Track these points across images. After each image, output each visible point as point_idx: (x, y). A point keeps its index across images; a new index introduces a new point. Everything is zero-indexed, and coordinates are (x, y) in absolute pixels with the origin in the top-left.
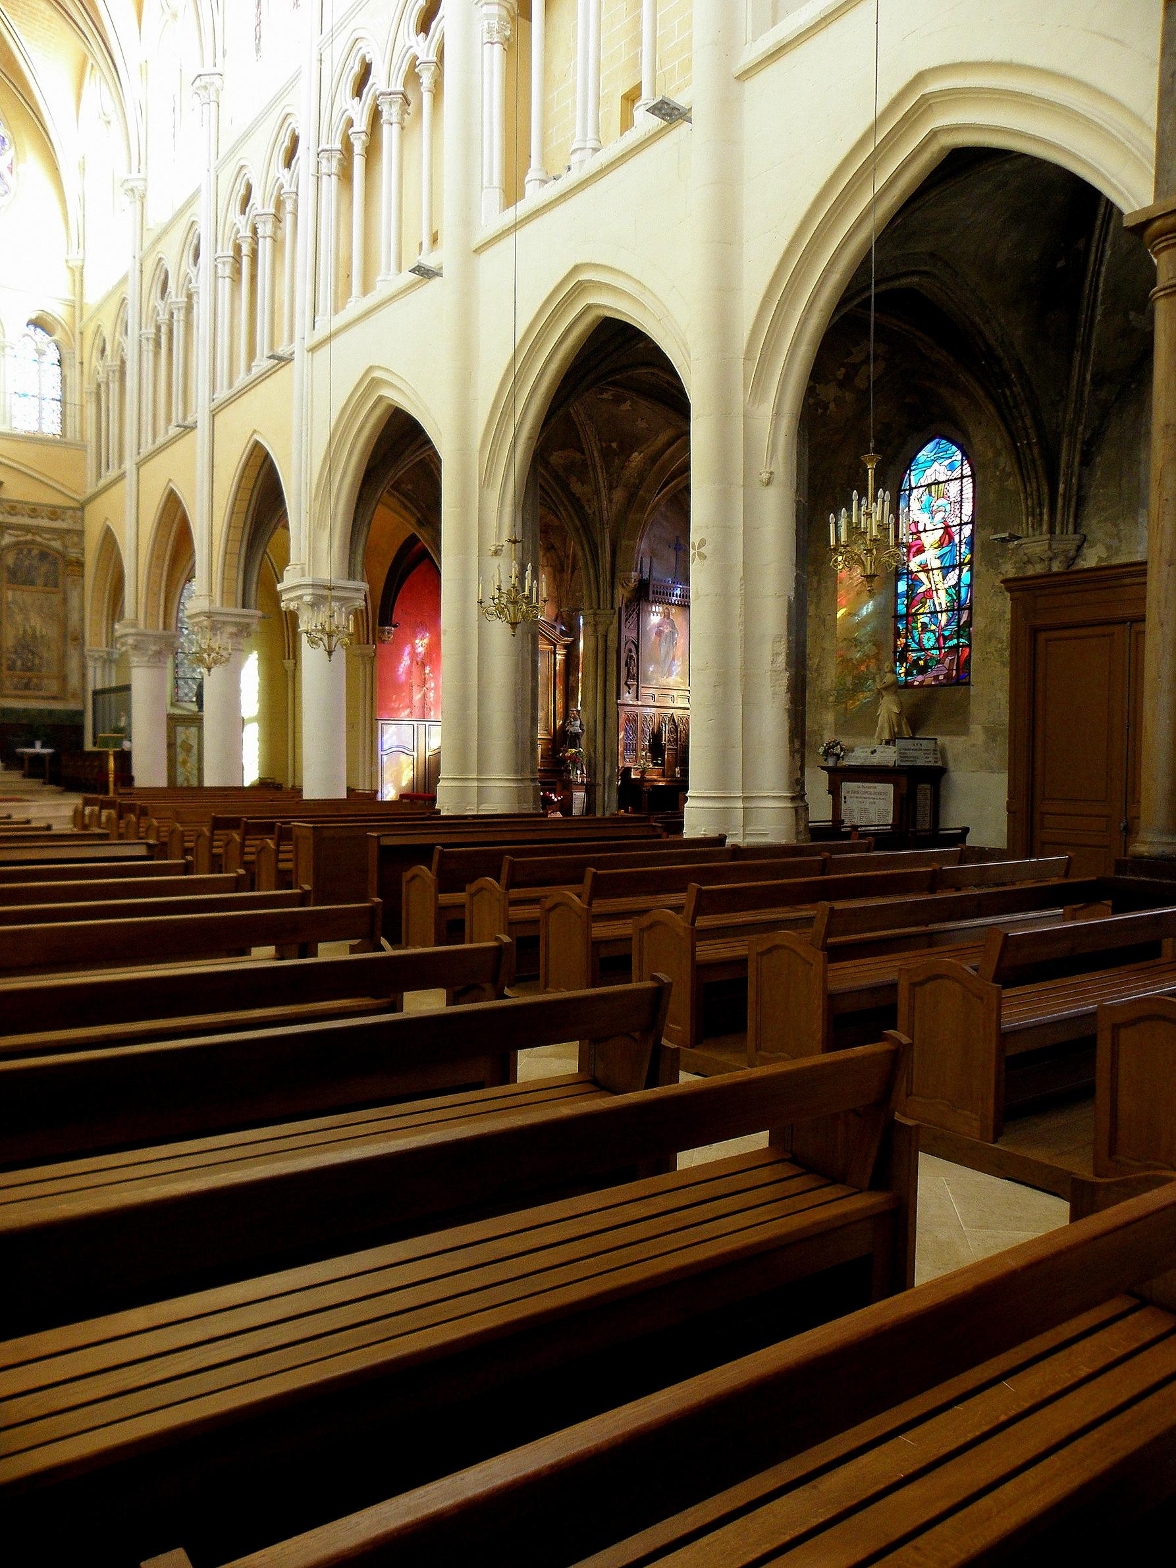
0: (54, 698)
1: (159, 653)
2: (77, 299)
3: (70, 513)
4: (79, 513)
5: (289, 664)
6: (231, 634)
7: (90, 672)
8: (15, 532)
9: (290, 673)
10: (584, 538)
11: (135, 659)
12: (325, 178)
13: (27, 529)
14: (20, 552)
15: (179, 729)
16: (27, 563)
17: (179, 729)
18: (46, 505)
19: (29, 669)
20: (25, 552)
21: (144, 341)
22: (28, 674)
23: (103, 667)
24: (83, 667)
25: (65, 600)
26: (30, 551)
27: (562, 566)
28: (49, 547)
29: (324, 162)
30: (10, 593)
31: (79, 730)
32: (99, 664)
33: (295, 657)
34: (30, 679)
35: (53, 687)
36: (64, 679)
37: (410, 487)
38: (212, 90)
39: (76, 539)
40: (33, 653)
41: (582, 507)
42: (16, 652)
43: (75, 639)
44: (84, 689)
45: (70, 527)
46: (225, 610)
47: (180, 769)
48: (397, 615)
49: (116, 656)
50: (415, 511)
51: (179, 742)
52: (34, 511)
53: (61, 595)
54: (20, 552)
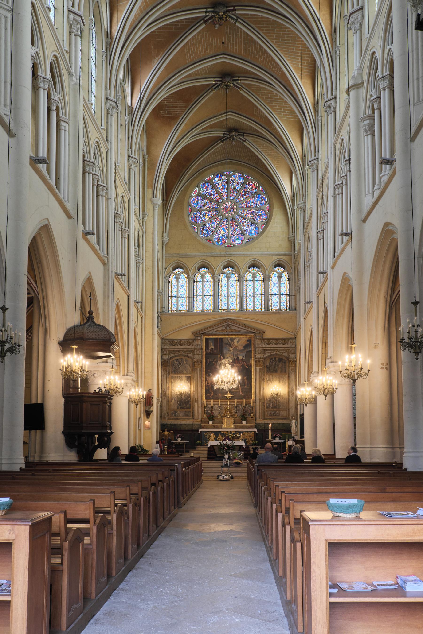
2: (293, 253)
3: (290, 340)
4: (294, 340)
12: (337, 196)
14: (272, 359)
16: (274, 363)
20: (273, 359)
21: (306, 267)
26: (275, 358)
28: (283, 355)
29: (337, 190)
38: (315, 165)
52: (277, 341)
54: (272, 359)
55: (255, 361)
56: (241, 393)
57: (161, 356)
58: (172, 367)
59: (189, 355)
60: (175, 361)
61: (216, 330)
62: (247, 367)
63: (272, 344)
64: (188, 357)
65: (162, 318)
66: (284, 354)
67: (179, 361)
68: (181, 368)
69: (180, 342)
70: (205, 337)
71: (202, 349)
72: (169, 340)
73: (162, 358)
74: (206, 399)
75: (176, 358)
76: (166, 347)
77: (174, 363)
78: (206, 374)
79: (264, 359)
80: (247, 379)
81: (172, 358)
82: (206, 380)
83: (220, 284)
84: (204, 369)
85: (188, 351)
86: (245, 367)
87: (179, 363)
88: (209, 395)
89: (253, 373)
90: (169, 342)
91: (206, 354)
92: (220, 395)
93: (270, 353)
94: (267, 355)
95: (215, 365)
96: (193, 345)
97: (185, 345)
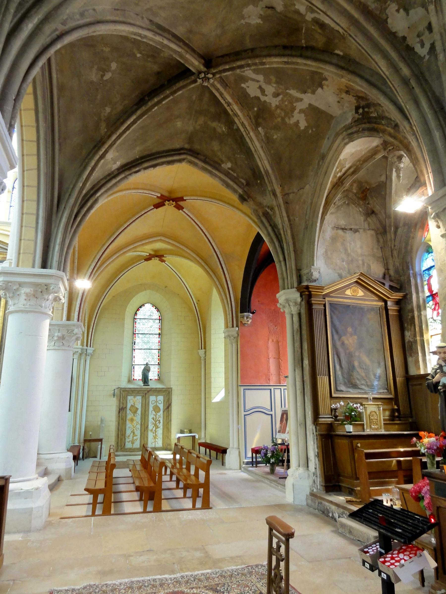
1: (63, 338)
5: (201, 352)
6: (27, 294)
9: (202, 358)
10: (417, 90)
15: (129, 398)
17: (129, 398)
27: (384, 228)
32: (76, 356)
33: (205, 348)
37: (229, 165)
41: (410, 49)
46: (20, 270)
47: (129, 424)
48: (255, 303)
50: (235, 186)
51: (129, 406)
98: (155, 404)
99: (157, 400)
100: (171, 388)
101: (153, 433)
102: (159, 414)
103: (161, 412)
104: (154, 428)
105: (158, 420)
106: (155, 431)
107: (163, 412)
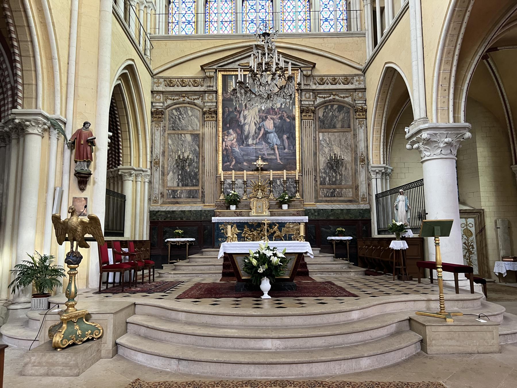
0: (350, 201)
3: (356, 78)
4: (362, 78)
7: (374, 181)
8: (323, 96)
11: (428, 154)
13: (330, 92)
18: (341, 76)
19: (334, 183)
20: (329, 107)
22: (334, 186)
23: (382, 179)
24: (369, 179)
25: (355, 135)
26: (332, 106)
30: (321, 134)
31: (369, 222)
32: (379, 176)
34: (334, 189)
35: (349, 194)
36: (357, 188)
39: (360, 95)
40: (336, 173)
42: (325, 172)
43: (363, 161)
44: (370, 195)
45: (357, 87)
49: (389, 171)
53: (352, 133)
55: (302, 112)
56: (279, 161)
57: (152, 103)
58: (169, 120)
59: (196, 101)
60: (174, 111)
61: (238, 63)
62: (288, 120)
63: (328, 84)
64: (195, 105)
65: (154, 43)
66: (346, 99)
67: (180, 112)
68: (183, 122)
69: (183, 82)
70: (223, 73)
71: (216, 92)
72: (165, 79)
73: (153, 106)
74: (224, 169)
75: (175, 106)
76: (161, 89)
77: (173, 114)
78: (223, 131)
79: (315, 108)
80: (288, 138)
81: (168, 106)
82: (223, 140)
83: (244, 4)
84: (221, 124)
85: (195, 95)
86: (285, 120)
87: (181, 114)
88: (228, 163)
89: (297, 129)
90: (165, 81)
91: (223, 100)
92: (245, 164)
93: (324, 98)
94: (319, 101)
95: (238, 117)
96: (202, 86)
97: (189, 86)
98: (465, 228)
99: (467, 223)
100: (483, 210)
101: (467, 259)
102: (471, 238)
103: (474, 236)
104: (468, 254)
105: (470, 246)
106: (469, 256)
107: (476, 236)
